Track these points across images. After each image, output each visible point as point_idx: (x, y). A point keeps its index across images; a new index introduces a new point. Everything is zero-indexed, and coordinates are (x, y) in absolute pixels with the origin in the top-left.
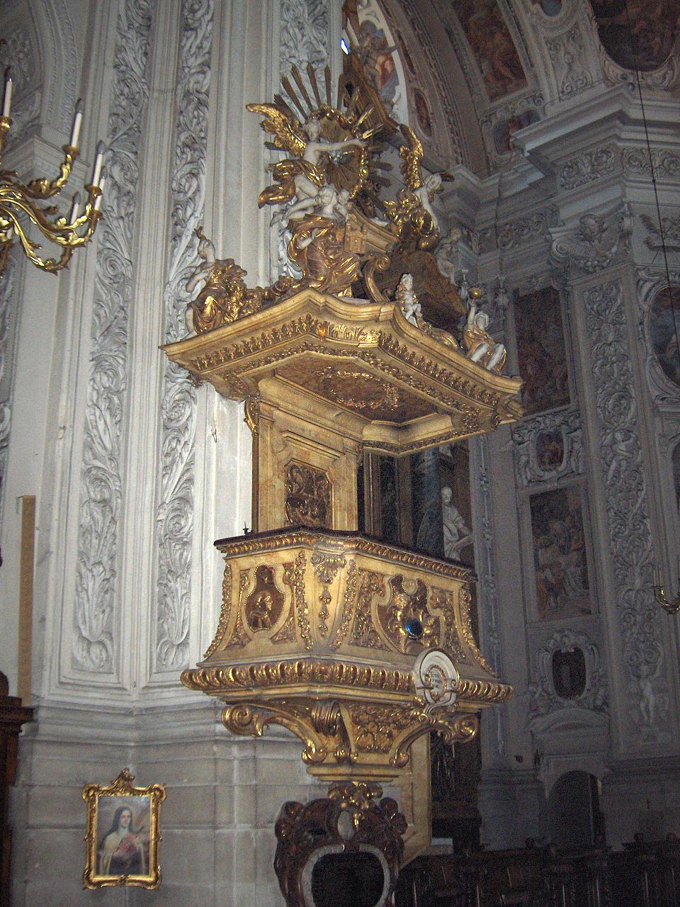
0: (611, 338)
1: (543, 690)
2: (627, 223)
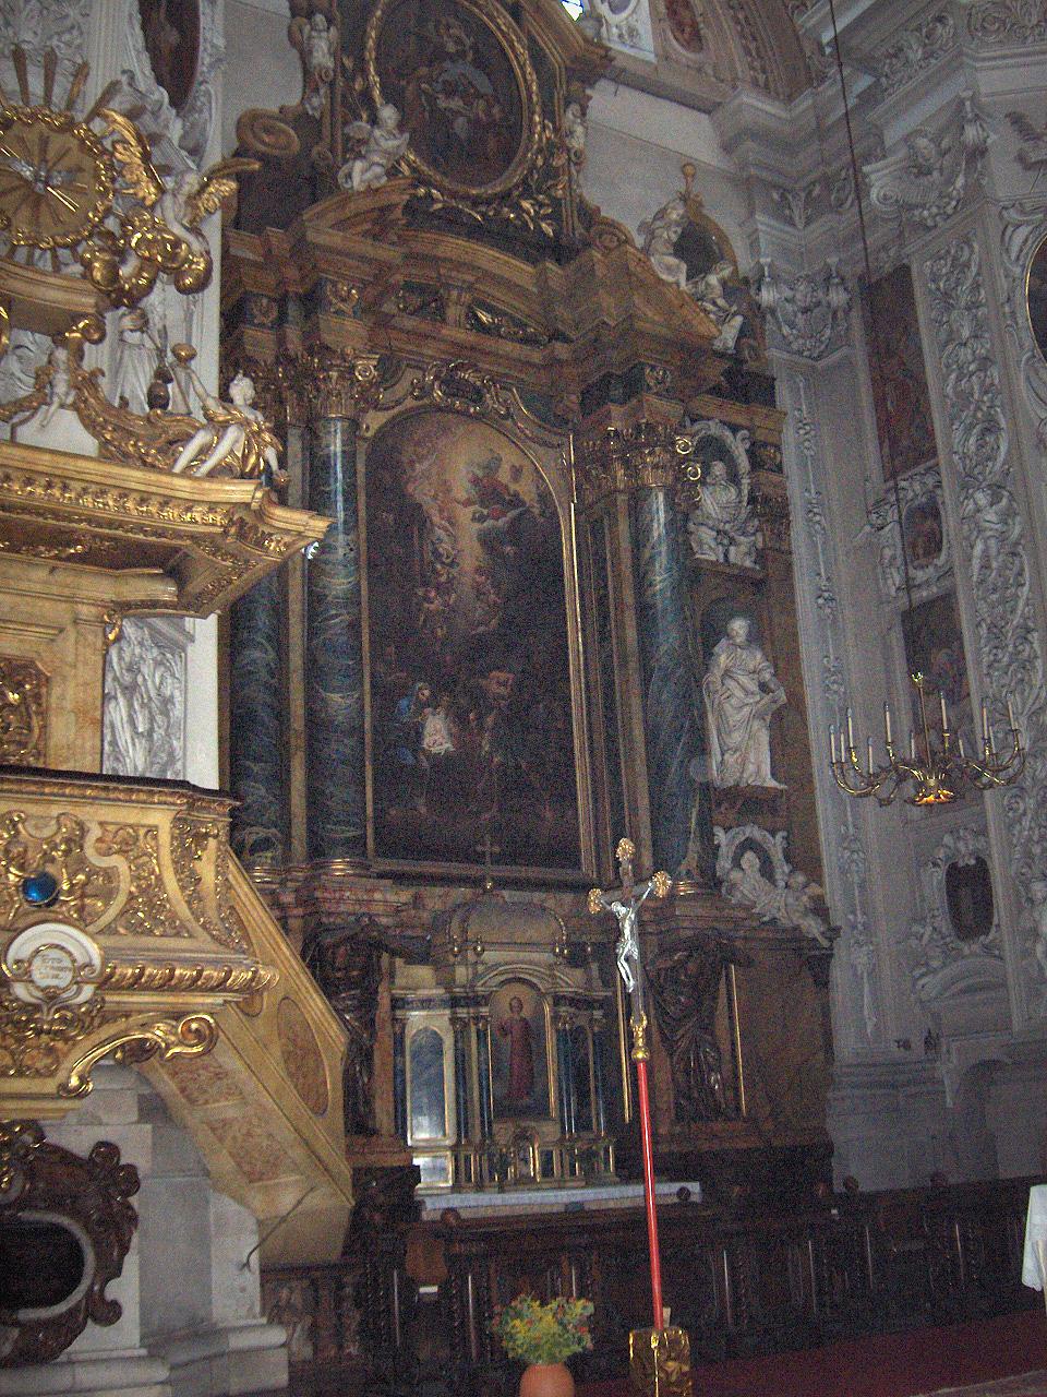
0: (966, 333)
1: (935, 929)
2: (971, 133)
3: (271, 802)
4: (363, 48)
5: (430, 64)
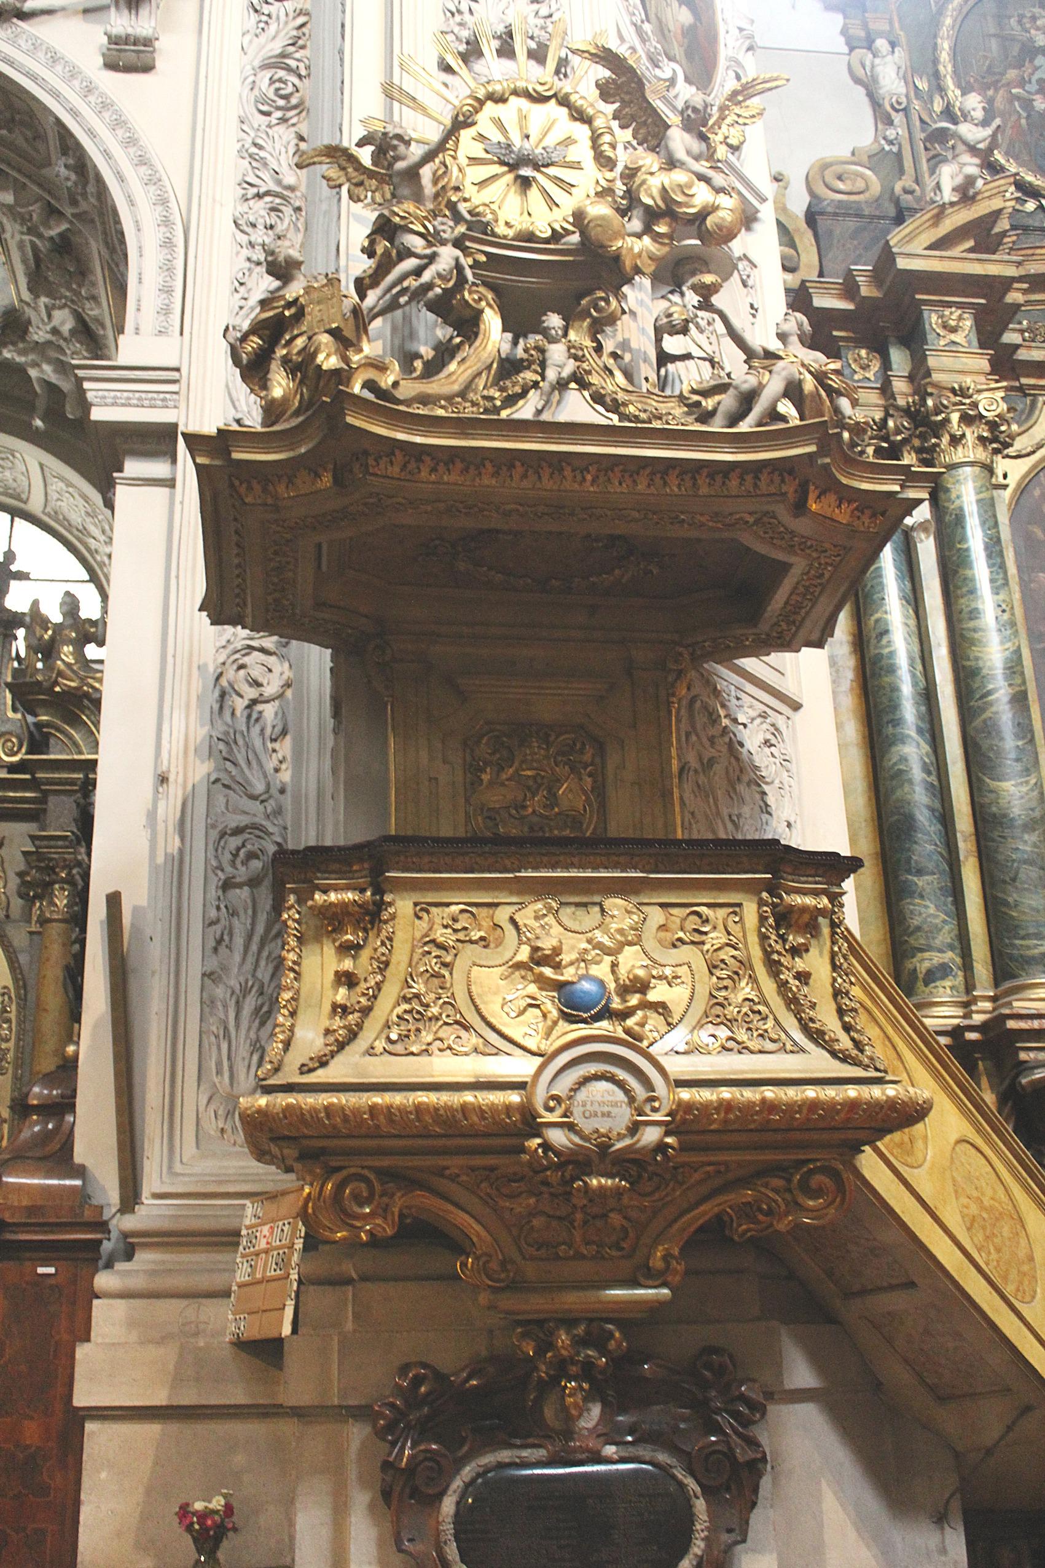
3: (944, 921)
4: (936, 61)
5: (1020, 66)
